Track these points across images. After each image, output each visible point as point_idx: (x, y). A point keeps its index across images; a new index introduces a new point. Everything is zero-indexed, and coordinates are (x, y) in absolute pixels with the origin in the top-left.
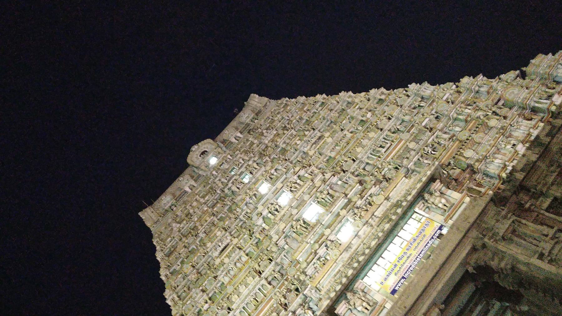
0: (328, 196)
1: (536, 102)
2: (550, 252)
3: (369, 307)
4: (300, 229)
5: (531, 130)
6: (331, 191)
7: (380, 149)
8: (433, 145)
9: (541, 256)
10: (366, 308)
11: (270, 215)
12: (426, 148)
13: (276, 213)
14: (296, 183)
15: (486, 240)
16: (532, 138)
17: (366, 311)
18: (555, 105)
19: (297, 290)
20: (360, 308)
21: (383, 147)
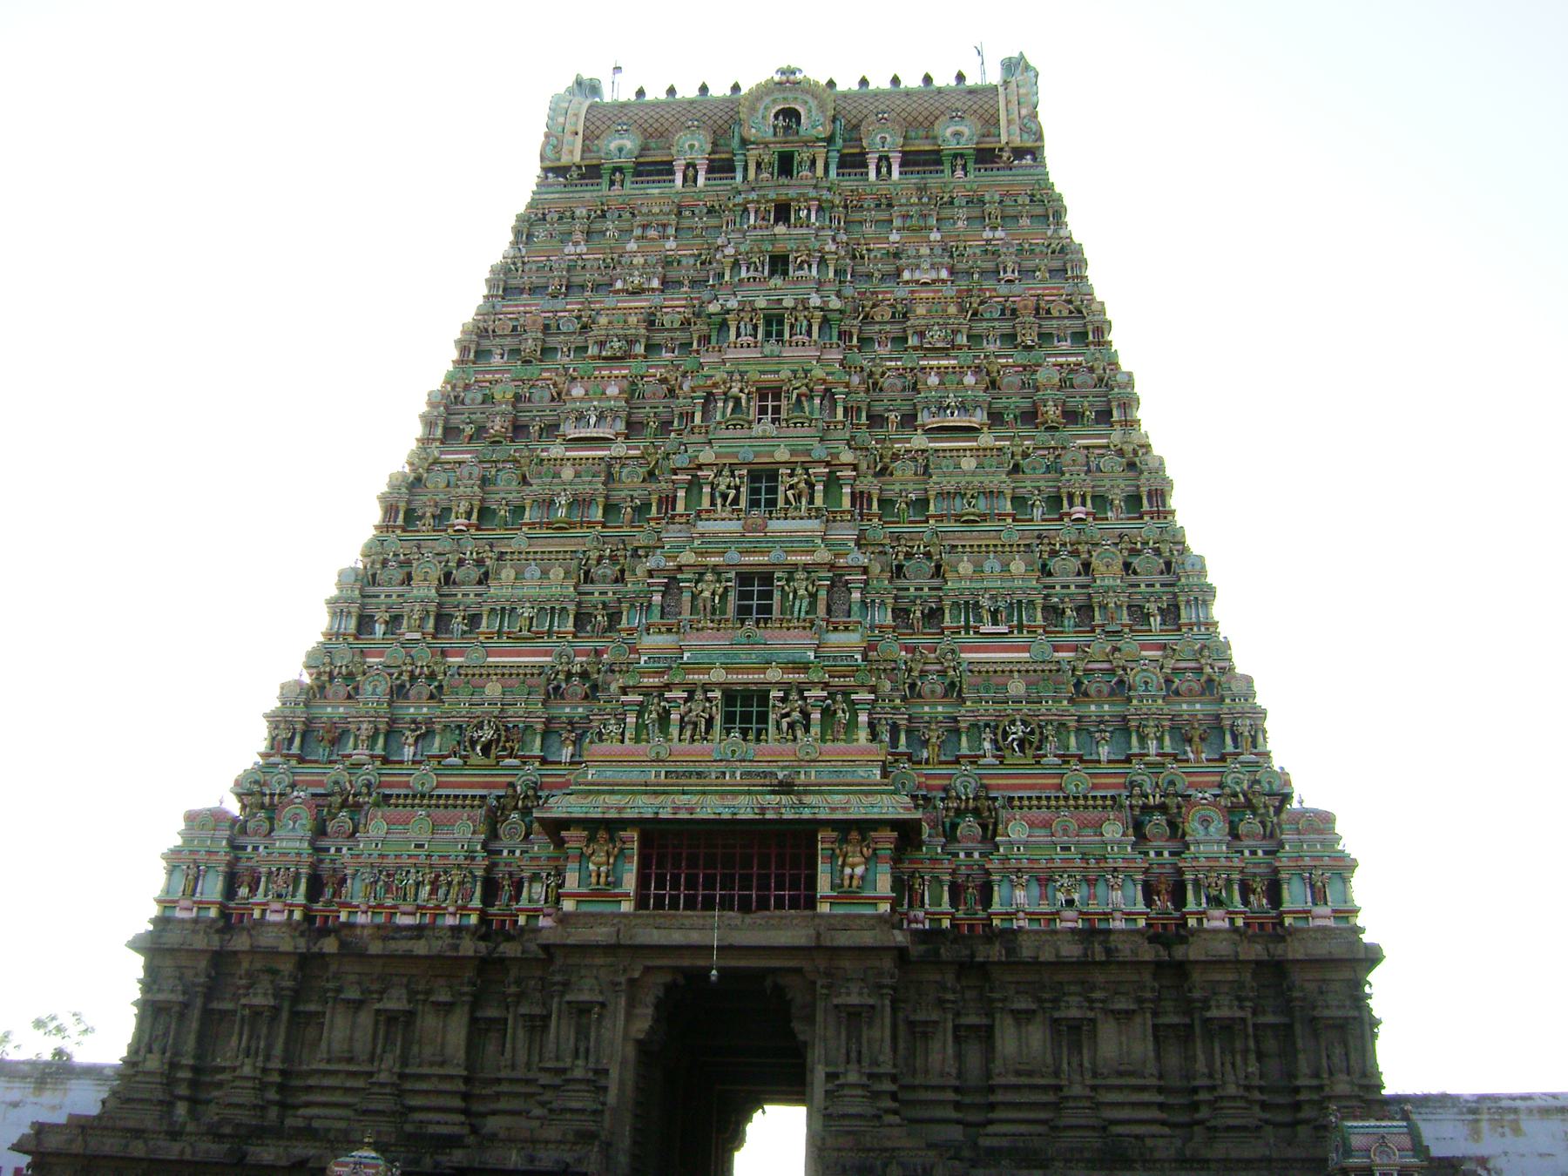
0: (805, 603)
1: (1196, 882)
2: (842, 1086)
3: (602, 880)
4: (705, 600)
5: (1117, 915)
6: (823, 594)
7: (986, 616)
8: (1032, 732)
9: (831, 1076)
10: (599, 876)
11: (707, 490)
13: (719, 501)
14: (811, 486)
16: (1103, 925)
17: (594, 880)
18: (1200, 921)
19: (595, 687)
20: (591, 867)
21: (995, 623)
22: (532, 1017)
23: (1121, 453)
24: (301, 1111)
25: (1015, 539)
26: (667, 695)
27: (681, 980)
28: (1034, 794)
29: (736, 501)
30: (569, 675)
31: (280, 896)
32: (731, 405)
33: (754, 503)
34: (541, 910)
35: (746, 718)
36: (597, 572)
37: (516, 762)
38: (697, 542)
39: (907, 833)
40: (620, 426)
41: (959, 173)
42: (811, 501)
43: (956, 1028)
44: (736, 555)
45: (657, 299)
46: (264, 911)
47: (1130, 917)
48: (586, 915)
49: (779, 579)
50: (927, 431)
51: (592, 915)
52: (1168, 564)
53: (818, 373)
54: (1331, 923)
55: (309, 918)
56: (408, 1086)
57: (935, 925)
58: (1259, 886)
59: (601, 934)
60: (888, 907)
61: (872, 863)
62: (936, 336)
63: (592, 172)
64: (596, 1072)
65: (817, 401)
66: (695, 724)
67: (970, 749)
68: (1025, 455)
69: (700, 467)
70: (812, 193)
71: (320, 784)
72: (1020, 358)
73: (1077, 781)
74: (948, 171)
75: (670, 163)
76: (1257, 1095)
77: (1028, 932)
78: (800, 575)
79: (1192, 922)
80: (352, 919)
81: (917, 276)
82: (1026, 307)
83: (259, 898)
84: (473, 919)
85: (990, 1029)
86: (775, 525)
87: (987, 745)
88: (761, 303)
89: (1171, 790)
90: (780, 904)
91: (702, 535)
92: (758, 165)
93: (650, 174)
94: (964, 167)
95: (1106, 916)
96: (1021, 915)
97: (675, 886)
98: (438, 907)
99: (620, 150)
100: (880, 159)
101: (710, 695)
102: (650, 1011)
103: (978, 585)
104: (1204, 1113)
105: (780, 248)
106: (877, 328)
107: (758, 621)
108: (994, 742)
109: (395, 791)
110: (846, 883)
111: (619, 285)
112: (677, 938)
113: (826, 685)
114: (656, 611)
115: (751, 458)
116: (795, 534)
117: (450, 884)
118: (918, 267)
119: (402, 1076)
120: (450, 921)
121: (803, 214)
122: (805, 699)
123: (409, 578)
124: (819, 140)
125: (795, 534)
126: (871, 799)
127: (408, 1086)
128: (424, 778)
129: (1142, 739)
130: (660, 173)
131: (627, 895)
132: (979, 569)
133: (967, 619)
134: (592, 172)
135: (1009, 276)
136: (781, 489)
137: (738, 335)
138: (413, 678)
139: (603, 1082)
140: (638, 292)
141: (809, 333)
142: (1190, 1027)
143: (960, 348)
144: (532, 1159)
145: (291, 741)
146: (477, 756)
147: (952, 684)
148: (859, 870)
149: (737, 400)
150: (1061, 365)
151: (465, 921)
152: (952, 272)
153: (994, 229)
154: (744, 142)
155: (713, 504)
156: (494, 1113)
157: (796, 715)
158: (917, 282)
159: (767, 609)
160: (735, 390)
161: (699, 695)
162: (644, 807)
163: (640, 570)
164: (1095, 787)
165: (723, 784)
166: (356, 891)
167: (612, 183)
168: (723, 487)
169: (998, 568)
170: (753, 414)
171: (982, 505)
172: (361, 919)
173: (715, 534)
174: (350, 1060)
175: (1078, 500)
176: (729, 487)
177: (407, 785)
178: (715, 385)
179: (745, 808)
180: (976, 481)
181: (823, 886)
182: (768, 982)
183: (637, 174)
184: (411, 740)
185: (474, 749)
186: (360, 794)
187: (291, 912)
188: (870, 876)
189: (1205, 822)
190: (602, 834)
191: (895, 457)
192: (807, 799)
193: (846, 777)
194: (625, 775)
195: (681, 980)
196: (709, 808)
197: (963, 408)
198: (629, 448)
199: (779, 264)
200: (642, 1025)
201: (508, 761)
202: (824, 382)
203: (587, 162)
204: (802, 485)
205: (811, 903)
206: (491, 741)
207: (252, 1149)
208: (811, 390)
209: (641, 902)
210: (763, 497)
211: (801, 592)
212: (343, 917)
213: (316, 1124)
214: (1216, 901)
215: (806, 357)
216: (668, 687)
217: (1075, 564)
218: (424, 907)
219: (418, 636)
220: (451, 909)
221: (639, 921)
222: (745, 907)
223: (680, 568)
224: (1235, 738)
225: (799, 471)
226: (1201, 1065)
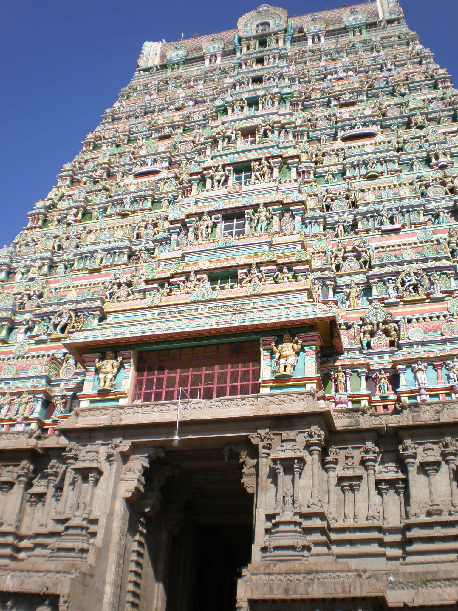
0: (265, 224)
3: (108, 383)
12: (412, 274)
13: (216, 184)
15: (260, 445)
26: (171, 280)
30: (119, 285)
32: (226, 140)
36: (143, 232)
40: (166, 164)
41: (358, 33)
49: (248, 214)
57: (356, 406)
59: (100, 420)
60: (314, 386)
61: (302, 354)
62: (347, 98)
69: (205, 169)
72: (398, 100)
75: (203, 57)
77: (429, 404)
78: (262, 209)
84: (34, 426)
85: (406, 481)
87: (391, 291)
88: (246, 96)
90: (234, 391)
94: (360, 32)
96: (423, 391)
98: (11, 420)
99: (177, 56)
100: (314, 36)
101: (199, 276)
105: (257, 74)
110: (282, 369)
113: (274, 262)
122: (260, 271)
126: (297, 309)
131: (123, 393)
135: (389, 66)
136: (253, 174)
138: (30, 297)
139: (93, 528)
143: (362, 101)
146: (57, 334)
147: (365, 262)
149: (229, 138)
153: (378, 52)
159: (243, 233)
160: (228, 133)
167: (173, 69)
171: (379, 168)
176: (222, 176)
177: (10, 352)
178: (218, 133)
180: (375, 156)
184: (23, 330)
185: (55, 330)
190: (110, 353)
191: (324, 155)
195: (162, 455)
197: (365, 125)
199: (258, 80)
202: (279, 122)
204: (265, 169)
205: (256, 389)
208: (273, 127)
216: (173, 276)
221: (130, 410)
222: (208, 395)
223: (188, 216)
225: (263, 161)
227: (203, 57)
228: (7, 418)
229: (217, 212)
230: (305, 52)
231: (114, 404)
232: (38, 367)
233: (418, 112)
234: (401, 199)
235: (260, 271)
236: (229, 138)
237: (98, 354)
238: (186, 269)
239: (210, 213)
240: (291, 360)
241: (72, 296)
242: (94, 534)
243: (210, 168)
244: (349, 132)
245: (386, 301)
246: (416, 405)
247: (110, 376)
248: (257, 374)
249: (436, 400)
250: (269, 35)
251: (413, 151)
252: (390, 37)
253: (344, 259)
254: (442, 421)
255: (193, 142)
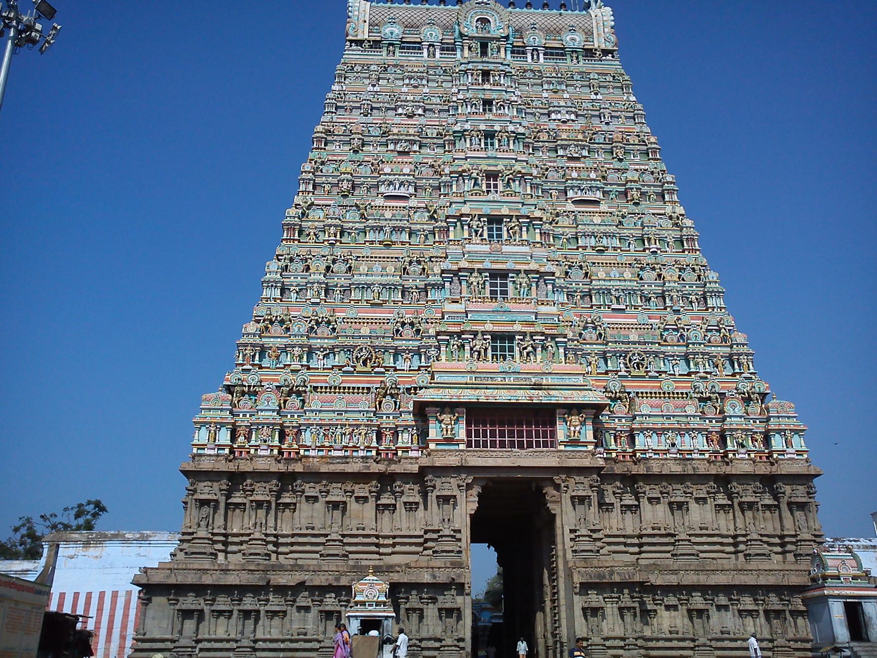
7: (614, 300)
8: (643, 360)
9: (572, 531)
13: (474, 234)
14: (521, 229)
15: (563, 485)
20: (443, 426)
21: (618, 303)
22: (411, 503)
23: (671, 218)
24: (290, 556)
25: (624, 261)
27: (490, 484)
28: (649, 391)
29: (481, 235)
31: (265, 441)
33: (490, 236)
34: (410, 448)
35: (503, 349)
36: (411, 269)
37: (383, 370)
38: (466, 256)
39: (598, 408)
40: (411, 190)
41: (575, 61)
42: (521, 236)
43: (622, 506)
44: (489, 264)
45: (422, 121)
46: (256, 450)
47: (702, 452)
48: (441, 451)
50: (574, 202)
51: (445, 451)
52: (699, 276)
53: (518, 167)
54: (795, 456)
55: (281, 453)
56: (346, 540)
57: (609, 456)
58: (759, 437)
59: (452, 460)
62: (573, 151)
63: (376, 44)
64: (455, 531)
65: (517, 182)
66: (479, 352)
67: (613, 367)
68: (623, 217)
70: (502, 68)
71: (277, 380)
73: (668, 385)
74: (569, 60)
76: (765, 539)
78: (523, 275)
79: (730, 455)
80: (307, 453)
81: (559, 116)
82: (617, 137)
83: (253, 443)
84: (374, 453)
85: (638, 506)
86: (505, 249)
87: (622, 365)
88: (482, 127)
89: (713, 390)
91: (469, 252)
92: (470, 48)
93: (408, 48)
94: (577, 58)
95: (690, 452)
97: (485, 436)
98: (354, 447)
99: (392, 33)
102: (477, 499)
103: (609, 283)
104: (742, 547)
106: (541, 144)
107: (504, 298)
108: (625, 364)
109: (319, 385)
111: (400, 111)
112: (491, 462)
113: (543, 334)
114: (448, 292)
115: (489, 212)
116: (514, 253)
117: (360, 434)
118: (560, 112)
119: (343, 536)
120: (361, 453)
121: (497, 78)
123: (308, 268)
124: (503, 37)
125: (514, 253)
127: (346, 540)
128: (336, 378)
129: (696, 364)
130: (414, 48)
132: (608, 274)
133: (604, 302)
134: (376, 44)
137: (471, 145)
138: (318, 323)
139: (458, 536)
140: (410, 116)
141: (508, 145)
142: (731, 506)
143: (585, 157)
144: (434, 577)
145: (254, 356)
147: (600, 334)
148: (578, 428)
149: (476, 179)
150: (637, 170)
151: (369, 454)
152: (577, 116)
153: (596, 94)
154: (461, 35)
155: (470, 235)
156: (393, 553)
157: (530, 349)
158: (559, 120)
160: (474, 175)
161: (480, 336)
162: (469, 396)
163: (437, 270)
164: (677, 388)
165: (506, 382)
166: (307, 438)
168: (475, 227)
169: (618, 275)
170: (484, 188)
172: (312, 453)
173: (476, 252)
174: (313, 528)
175: (653, 242)
178: (464, 171)
179: (522, 396)
181: (561, 435)
182: (534, 485)
183: (403, 48)
184: (321, 357)
186: (299, 386)
187: (272, 450)
188: (582, 431)
189: (734, 407)
191: (558, 215)
192: (552, 392)
193: (565, 379)
194: (460, 377)
195: (490, 484)
196: (503, 396)
198: (418, 202)
200: (474, 506)
201: (377, 370)
203: (373, 38)
206: (367, 359)
207: (272, 577)
209: (469, 444)
210: (495, 233)
211: (524, 284)
212: (302, 452)
213: (299, 562)
214: (743, 446)
215: (506, 157)
216: (463, 332)
217: (654, 274)
218: (347, 447)
219: (318, 301)
220: (362, 448)
223: (460, 270)
224: (739, 366)
225: (514, 219)
226: (740, 524)
227: (420, 43)
228: (351, 445)
229: (486, 270)
230: (525, 71)
231: (456, 447)
232: (365, 402)
233: (633, 185)
234: (625, 280)
235: (534, 340)
236: (476, 179)
237: (438, 409)
238: (475, 328)
239: (480, 271)
240: (578, 428)
241: (365, 330)
242: (460, 540)
243: (468, 215)
244: (580, 196)
245: (620, 373)
246: (646, 459)
247: (449, 427)
248: (553, 434)
249: (657, 456)
250: (493, 39)
251: (630, 229)
252: (606, 74)
253: (585, 328)
254: (663, 473)
255: (432, 166)
